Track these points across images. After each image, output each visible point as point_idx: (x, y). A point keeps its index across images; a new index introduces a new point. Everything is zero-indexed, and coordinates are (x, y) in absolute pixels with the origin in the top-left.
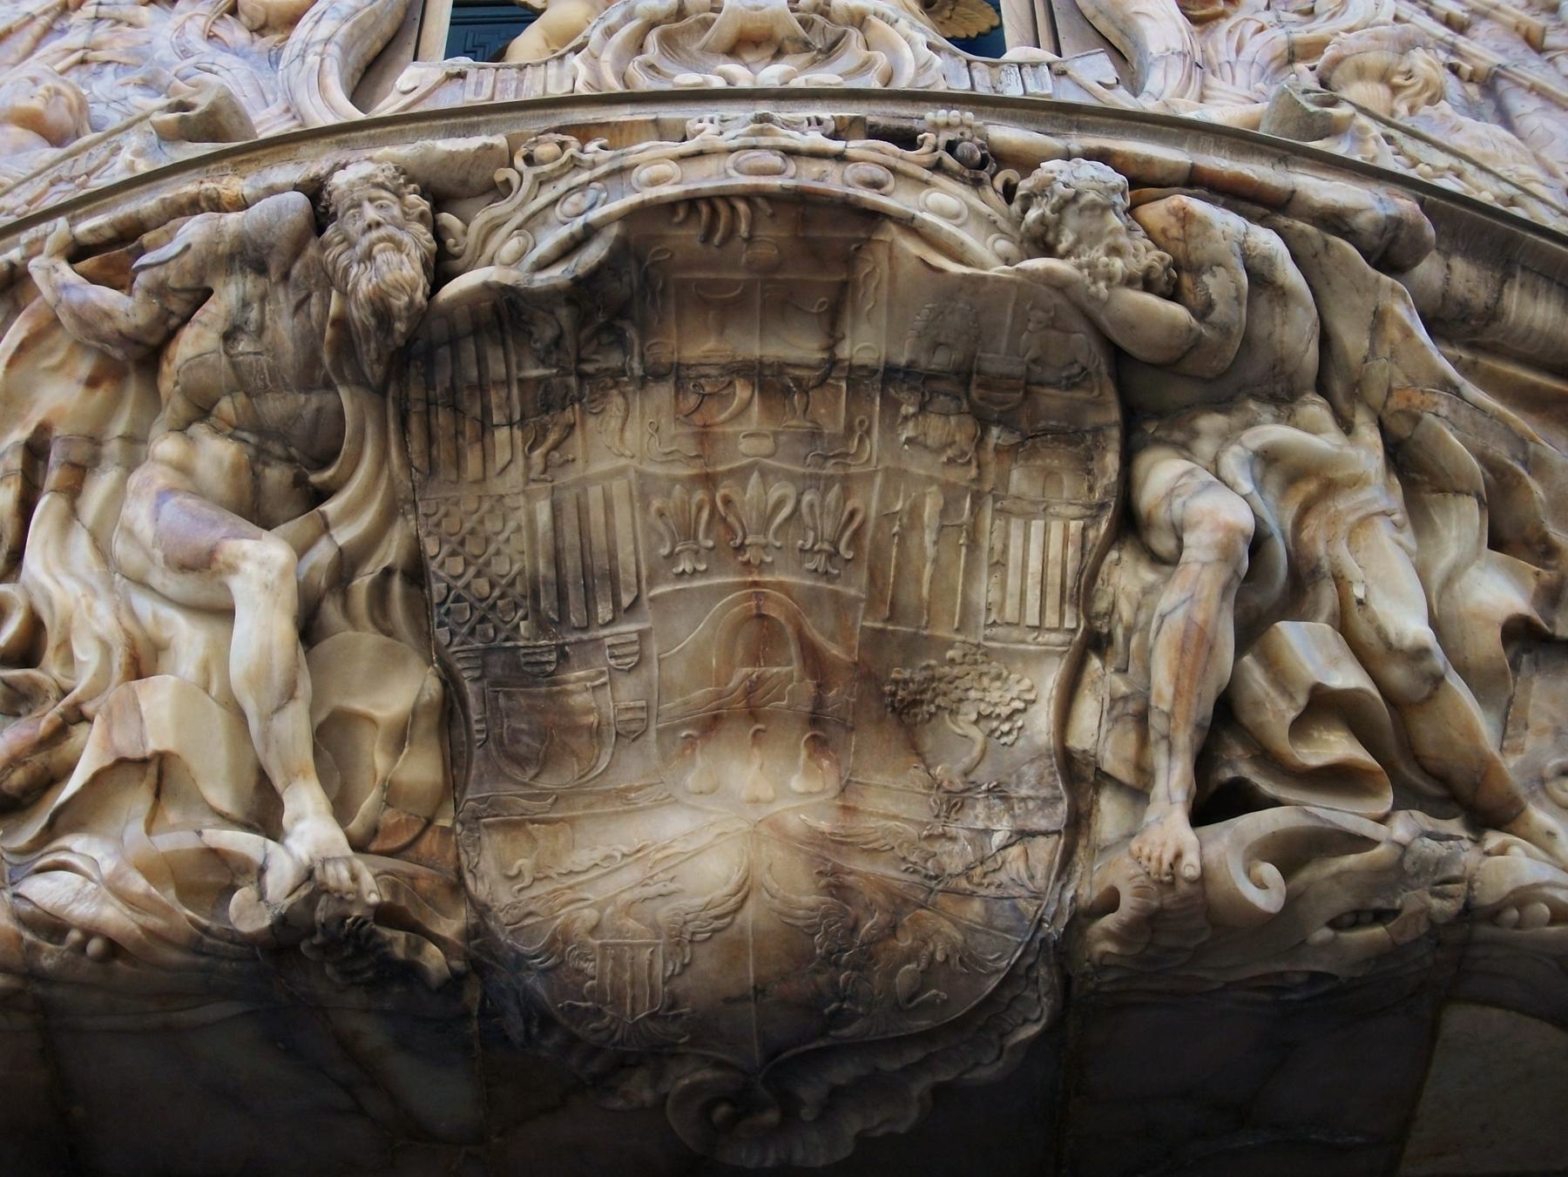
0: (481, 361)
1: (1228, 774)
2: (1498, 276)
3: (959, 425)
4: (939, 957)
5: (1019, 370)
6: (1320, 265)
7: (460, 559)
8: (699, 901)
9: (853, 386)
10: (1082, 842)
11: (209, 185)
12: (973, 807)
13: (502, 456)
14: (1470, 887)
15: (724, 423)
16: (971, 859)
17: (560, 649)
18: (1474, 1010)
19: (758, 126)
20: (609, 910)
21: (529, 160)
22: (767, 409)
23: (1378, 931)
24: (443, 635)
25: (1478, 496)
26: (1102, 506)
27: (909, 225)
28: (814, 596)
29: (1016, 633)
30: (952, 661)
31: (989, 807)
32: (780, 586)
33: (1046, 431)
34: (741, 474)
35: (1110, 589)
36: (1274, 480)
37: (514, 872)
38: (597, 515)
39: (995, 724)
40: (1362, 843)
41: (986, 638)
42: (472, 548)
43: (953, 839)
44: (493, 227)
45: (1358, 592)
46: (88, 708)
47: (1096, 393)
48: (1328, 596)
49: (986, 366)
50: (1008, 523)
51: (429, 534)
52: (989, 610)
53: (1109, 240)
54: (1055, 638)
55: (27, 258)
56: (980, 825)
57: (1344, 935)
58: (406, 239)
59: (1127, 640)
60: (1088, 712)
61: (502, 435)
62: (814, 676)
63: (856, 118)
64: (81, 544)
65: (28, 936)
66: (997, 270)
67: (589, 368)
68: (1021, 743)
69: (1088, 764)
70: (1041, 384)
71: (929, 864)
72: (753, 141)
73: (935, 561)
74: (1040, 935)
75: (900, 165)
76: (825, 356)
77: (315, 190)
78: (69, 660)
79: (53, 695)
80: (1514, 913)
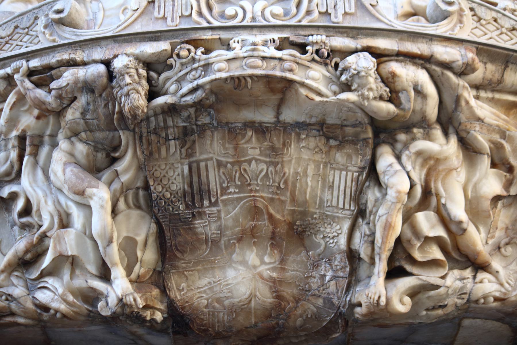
0: (165, 121)
1: (397, 264)
2: (503, 68)
3: (320, 140)
4: (309, 316)
5: (339, 122)
6: (440, 79)
7: (160, 186)
8: (237, 300)
9: (285, 130)
10: (354, 278)
11: (72, 56)
12: (321, 267)
13: (172, 150)
14: (469, 295)
15: (243, 144)
16: (319, 284)
17: (193, 213)
18: (472, 320)
19: (253, 47)
20: (210, 300)
21: (178, 55)
22: (258, 140)
23: (440, 312)
24: (156, 210)
25: (488, 154)
26: (364, 168)
27: (303, 85)
28: (272, 200)
29: (335, 210)
30: (316, 218)
31: (325, 267)
32: (262, 197)
33: (347, 141)
34: (249, 162)
35: (366, 196)
36: (420, 161)
37: (181, 288)
38: (203, 174)
39: (328, 239)
40: (437, 287)
41: (326, 211)
42: (165, 182)
43: (315, 277)
44: (168, 79)
45: (443, 201)
46: (48, 234)
47: (364, 129)
48: (434, 201)
49: (328, 122)
50: (334, 172)
51: (151, 178)
52: (327, 201)
53: (368, 86)
54: (348, 212)
55: (14, 74)
56: (322, 273)
57: (429, 313)
58: (140, 88)
59: (370, 216)
60: (357, 235)
61: (172, 142)
62: (272, 225)
63: (285, 38)
64: (40, 173)
65: (39, 311)
66: (332, 98)
67: (199, 123)
68: (336, 247)
69: (357, 253)
70: (346, 126)
71: (307, 286)
72: (250, 53)
73: (311, 187)
74: (339, 311)
75: (300, 61)
76: (276, 120)
77: (107, 63)
78: (40, 216)
79: (37, 227)
80: (482, 301)
